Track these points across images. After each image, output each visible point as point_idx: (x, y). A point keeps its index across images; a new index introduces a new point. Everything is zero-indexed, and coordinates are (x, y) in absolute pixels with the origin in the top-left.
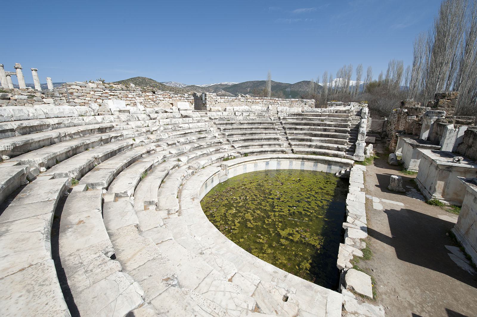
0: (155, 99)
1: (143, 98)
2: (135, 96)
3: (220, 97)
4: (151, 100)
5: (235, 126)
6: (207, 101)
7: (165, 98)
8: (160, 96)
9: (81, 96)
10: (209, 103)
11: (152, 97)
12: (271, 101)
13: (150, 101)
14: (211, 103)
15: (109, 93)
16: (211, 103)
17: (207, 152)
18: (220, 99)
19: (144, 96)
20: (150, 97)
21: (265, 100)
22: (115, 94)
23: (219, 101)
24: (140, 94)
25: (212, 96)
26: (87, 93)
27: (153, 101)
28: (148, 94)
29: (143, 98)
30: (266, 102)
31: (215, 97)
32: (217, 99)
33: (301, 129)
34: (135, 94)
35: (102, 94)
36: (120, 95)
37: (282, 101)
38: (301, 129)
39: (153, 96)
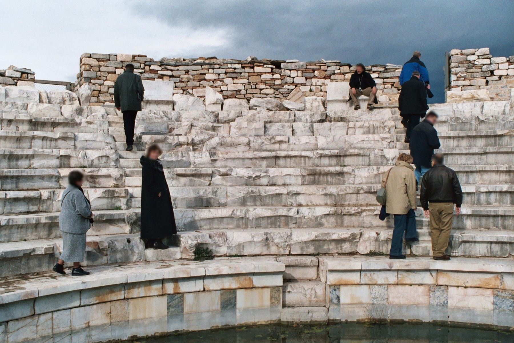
0: (278, 82)
1: (246, 81)
2: (222, 76)
3: (504, 59)
4: (266, 84)
6: (453, 77)
7: (311, 78)
8: (293, 74)
9: (94, 79)
10: (461, 83)
11: (270, 76)
13: (262, 86)
14: (467, 82)
15: (159, 72)
16: (467, 82)
18: (506, 65)
19: (247, 75)
20: (263, 76)
22: (175, 73)
23: (504, 73)
24: (236, 71)
25: (471, 58)
26: (109, 73)
27: (272, 86)
28: (257, 69)
29: (246, 81)
31: (487, 61)
32: (492, 67)
34: (223, 71)
35: (141, 73)
36: (186, 76)
39: (272, 73)
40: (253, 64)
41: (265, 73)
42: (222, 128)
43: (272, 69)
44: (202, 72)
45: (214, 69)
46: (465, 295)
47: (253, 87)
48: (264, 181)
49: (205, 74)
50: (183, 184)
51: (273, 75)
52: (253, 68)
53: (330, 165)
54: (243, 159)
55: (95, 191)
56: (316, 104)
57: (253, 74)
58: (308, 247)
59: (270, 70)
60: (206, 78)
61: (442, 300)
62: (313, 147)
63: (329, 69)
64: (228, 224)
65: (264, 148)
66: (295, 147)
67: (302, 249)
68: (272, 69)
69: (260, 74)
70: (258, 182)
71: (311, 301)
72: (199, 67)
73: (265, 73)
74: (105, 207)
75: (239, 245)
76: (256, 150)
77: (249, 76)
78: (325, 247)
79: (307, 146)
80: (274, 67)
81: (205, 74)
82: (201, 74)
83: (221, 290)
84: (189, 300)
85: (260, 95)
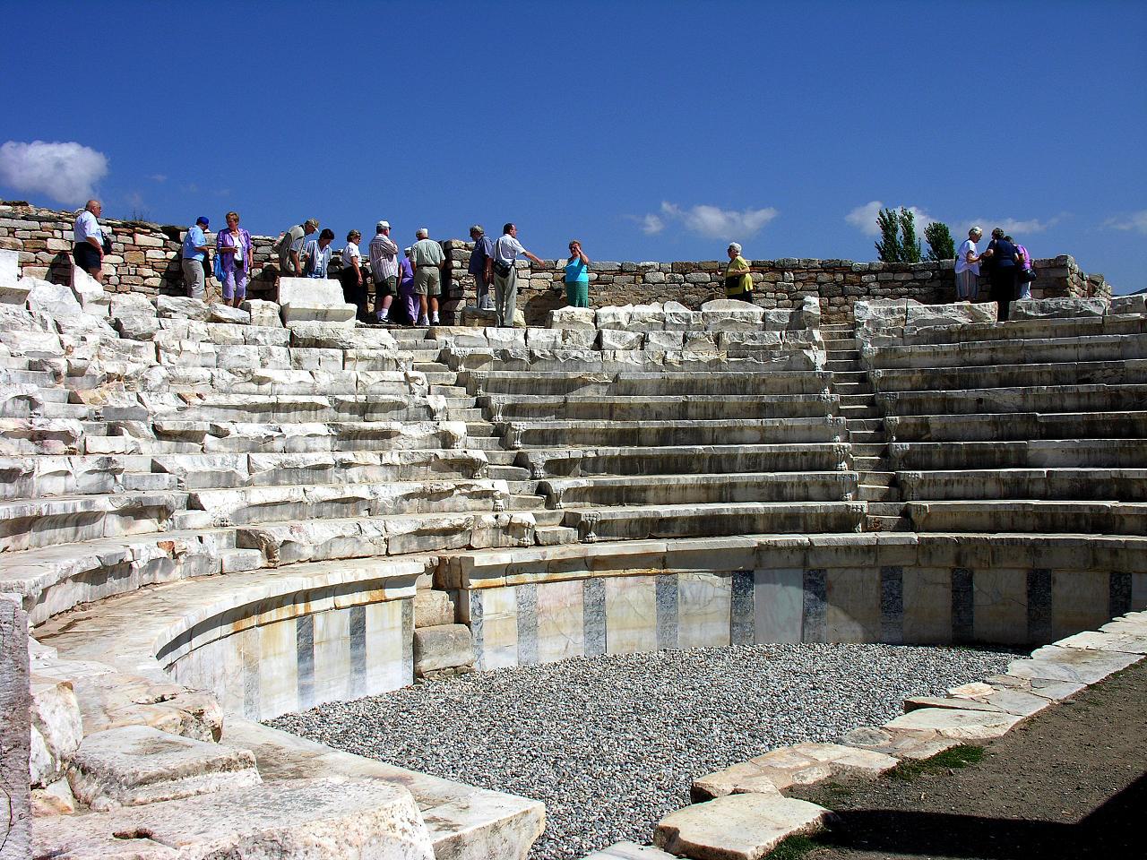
1: (119, 260)
5: (589, 394)
12: (825, 277)
13: (148, 272)
17: (369, 497)
19: (121, 247)
21: (790, 275)
23: (525, 283)
29: (119, 260)
30: (800, 285)
33: (980, 406)
37: (890, 276)
38: (980, 406)
39: (166, 248)
40: (133, 228)
41: (153, 248)
42: (144, 350)
43: (165, 240)
44: (41, 234)
45: (62, 231)
46: (624, 587)
47: (132, 272)
48: (278, 444)
49: (46, 239)
50: (167, 450)
51: (166, 252)
52: (129, 235)
53: (350, 420)
54: (226, 407)
55: (84, 460)
56: (268, 313)
57: (132, 247)
58: (410, 542)
59: (161, 243)
60: (49, 247)
61: (599, 595)
62: (310, 390)
63: (259, 250)
64: (281, 513)
65: (235, 388)
66: (285, 389)
67: (403, 544)
68: (165, 240)
69: (144, 249)
70: (269, 446)
71: (442, 618)
72: (35, 224)
73: (153, 248)
74: (94, 489)
75: (326, 543)
76: (222, 392)
77: (125, 251)
78: (431, 541)
79: (301, 388)
80: (167, 237)
81: (46, 239)
82: (39, 238)
83: (353, 606)
84: (319, 621)
85: (143, 289)
